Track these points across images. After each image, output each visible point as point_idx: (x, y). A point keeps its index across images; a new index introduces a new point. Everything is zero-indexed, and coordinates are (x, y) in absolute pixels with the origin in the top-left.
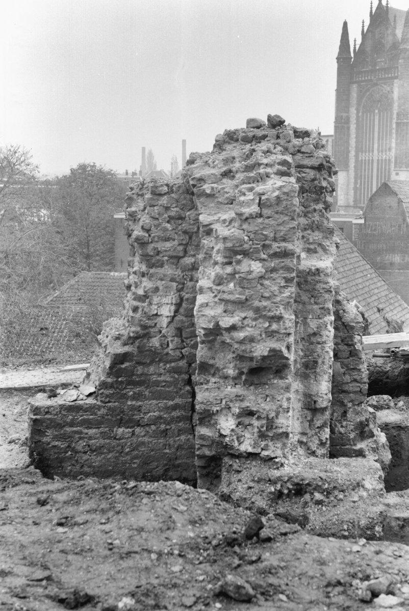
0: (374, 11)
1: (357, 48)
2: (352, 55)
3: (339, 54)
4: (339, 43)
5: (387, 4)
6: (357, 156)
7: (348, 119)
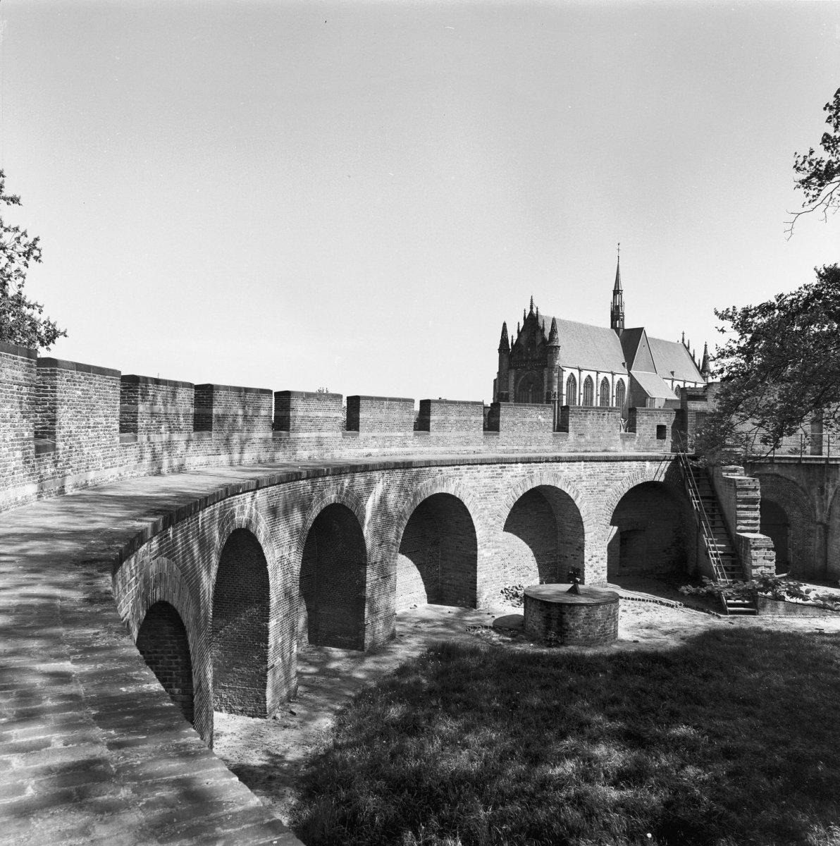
1: (514, 343)
2: (510, 347)
3: (501, 346)
4: (500, 338)
5: (537, 314)
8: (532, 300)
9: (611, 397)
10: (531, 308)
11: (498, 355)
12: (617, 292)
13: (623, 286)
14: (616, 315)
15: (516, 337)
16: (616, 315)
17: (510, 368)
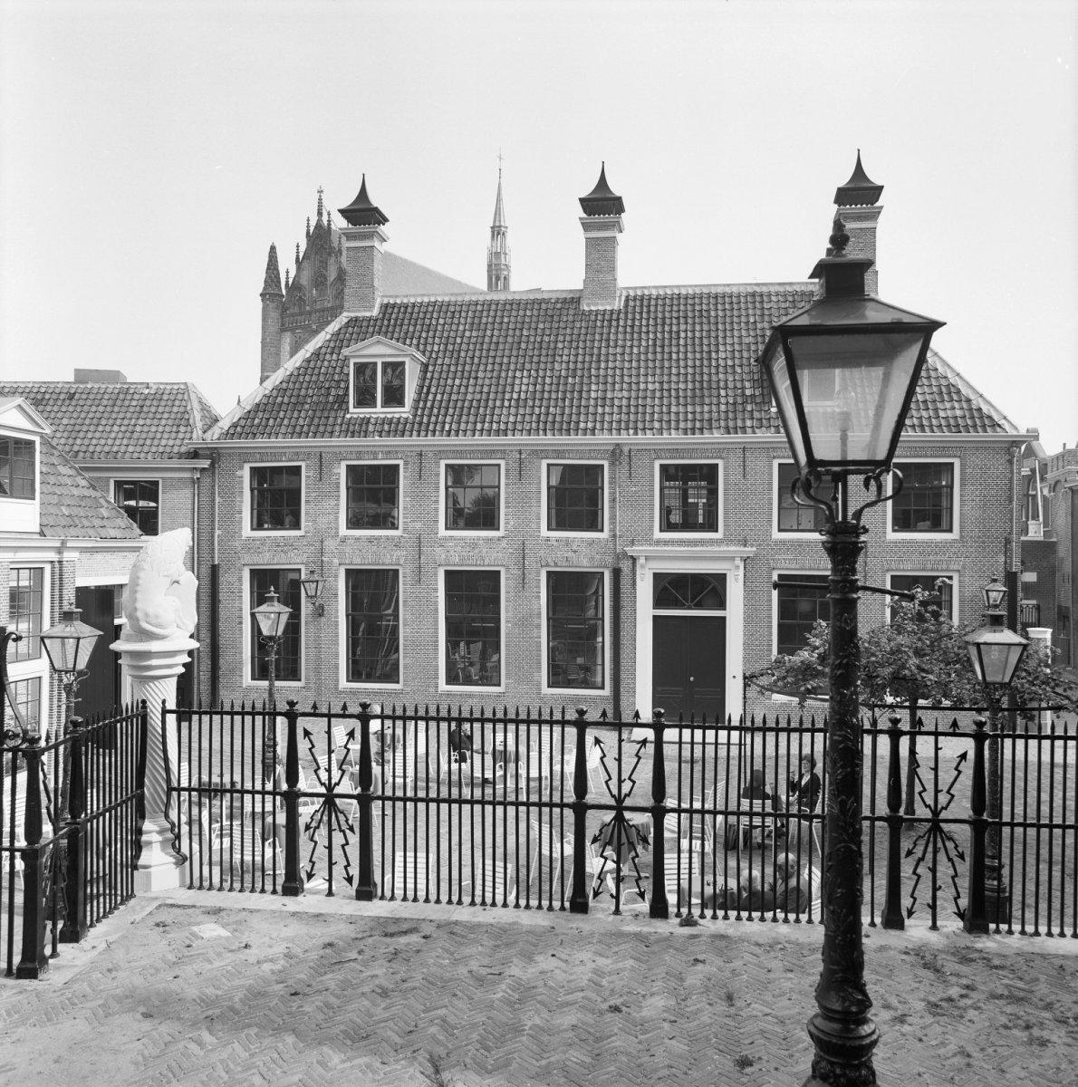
2: (284, 292)
5: (329, 224)
10: (320, 214)
12: (497, 231)
13: (508, 221)
14: (497, 273)
15: (292, 274)
16: (497, 273)
17: (283, 330)
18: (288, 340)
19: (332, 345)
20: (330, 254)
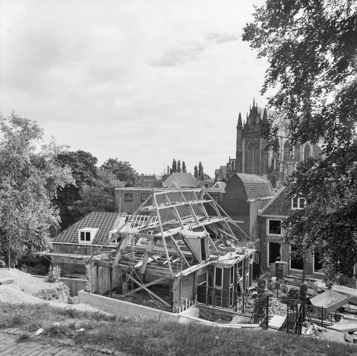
0: (251, 109)
3: (238, 126)
6: (245, 168)
7: (241, 152)
8: (254, 101)
9: (301, 153)
10: (254, 104)
11: (236, 130)
17: (243, 137)
18: (244, 140)
19: (286, 190)
20: (257, 115)
